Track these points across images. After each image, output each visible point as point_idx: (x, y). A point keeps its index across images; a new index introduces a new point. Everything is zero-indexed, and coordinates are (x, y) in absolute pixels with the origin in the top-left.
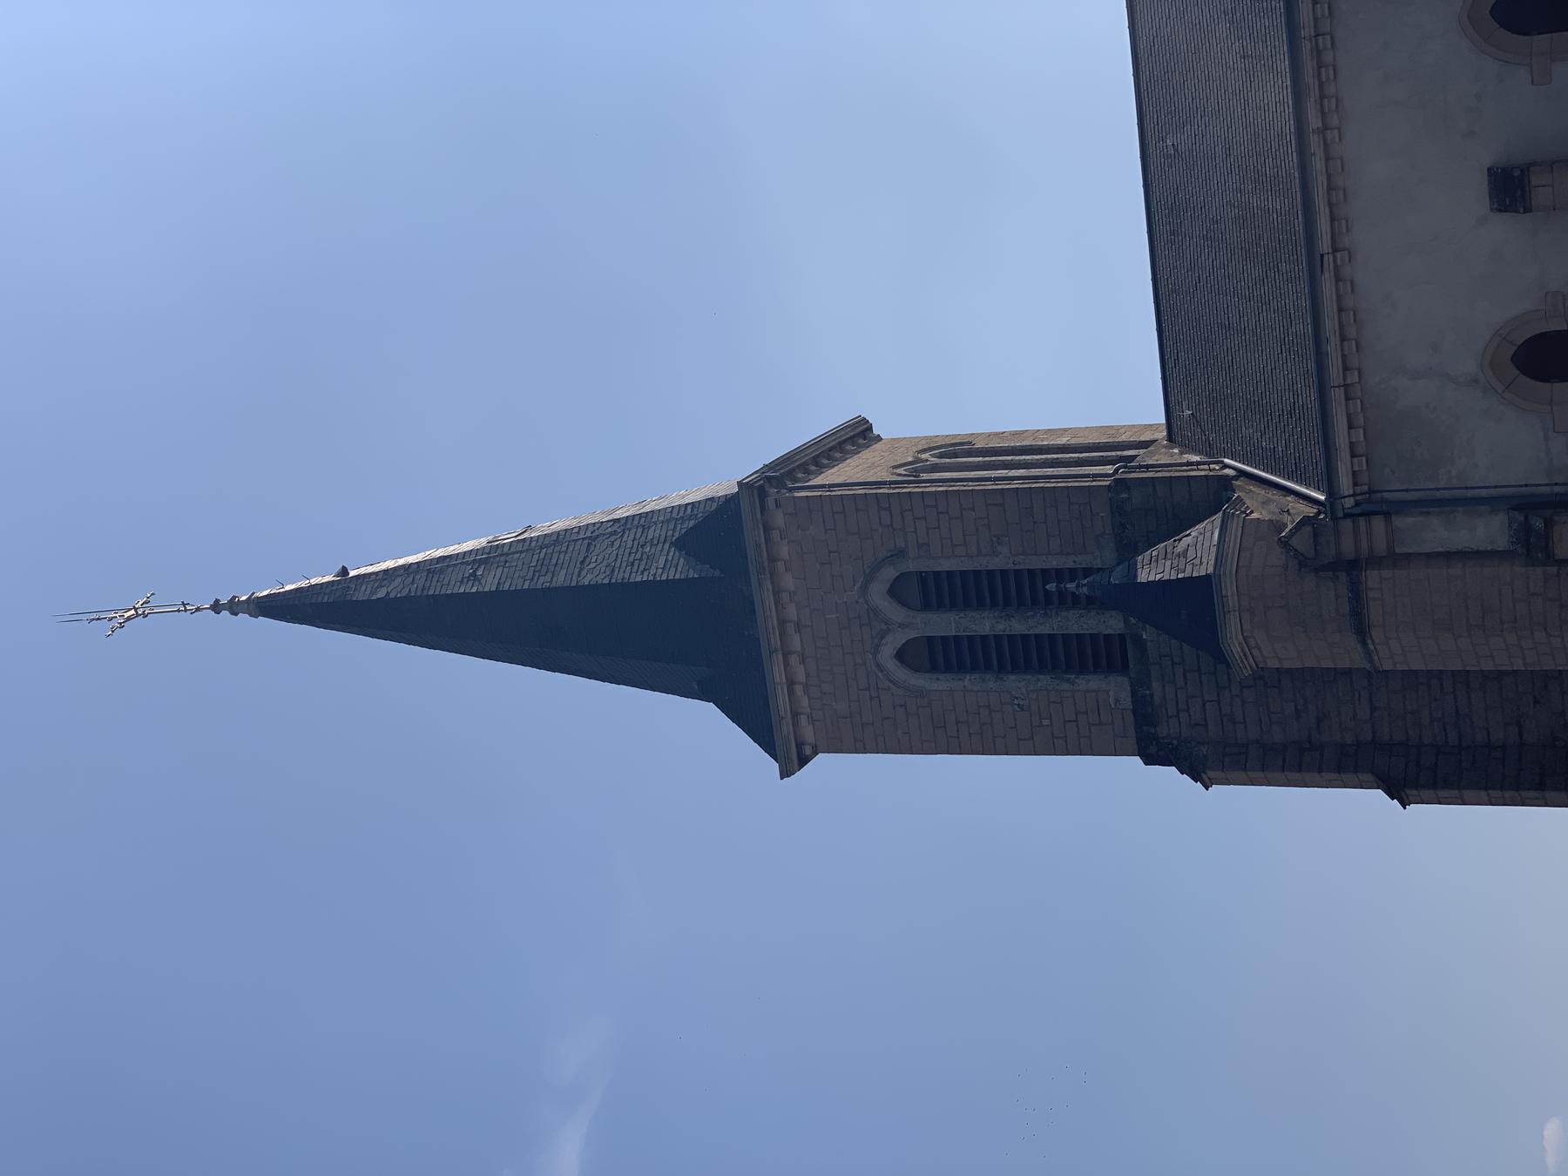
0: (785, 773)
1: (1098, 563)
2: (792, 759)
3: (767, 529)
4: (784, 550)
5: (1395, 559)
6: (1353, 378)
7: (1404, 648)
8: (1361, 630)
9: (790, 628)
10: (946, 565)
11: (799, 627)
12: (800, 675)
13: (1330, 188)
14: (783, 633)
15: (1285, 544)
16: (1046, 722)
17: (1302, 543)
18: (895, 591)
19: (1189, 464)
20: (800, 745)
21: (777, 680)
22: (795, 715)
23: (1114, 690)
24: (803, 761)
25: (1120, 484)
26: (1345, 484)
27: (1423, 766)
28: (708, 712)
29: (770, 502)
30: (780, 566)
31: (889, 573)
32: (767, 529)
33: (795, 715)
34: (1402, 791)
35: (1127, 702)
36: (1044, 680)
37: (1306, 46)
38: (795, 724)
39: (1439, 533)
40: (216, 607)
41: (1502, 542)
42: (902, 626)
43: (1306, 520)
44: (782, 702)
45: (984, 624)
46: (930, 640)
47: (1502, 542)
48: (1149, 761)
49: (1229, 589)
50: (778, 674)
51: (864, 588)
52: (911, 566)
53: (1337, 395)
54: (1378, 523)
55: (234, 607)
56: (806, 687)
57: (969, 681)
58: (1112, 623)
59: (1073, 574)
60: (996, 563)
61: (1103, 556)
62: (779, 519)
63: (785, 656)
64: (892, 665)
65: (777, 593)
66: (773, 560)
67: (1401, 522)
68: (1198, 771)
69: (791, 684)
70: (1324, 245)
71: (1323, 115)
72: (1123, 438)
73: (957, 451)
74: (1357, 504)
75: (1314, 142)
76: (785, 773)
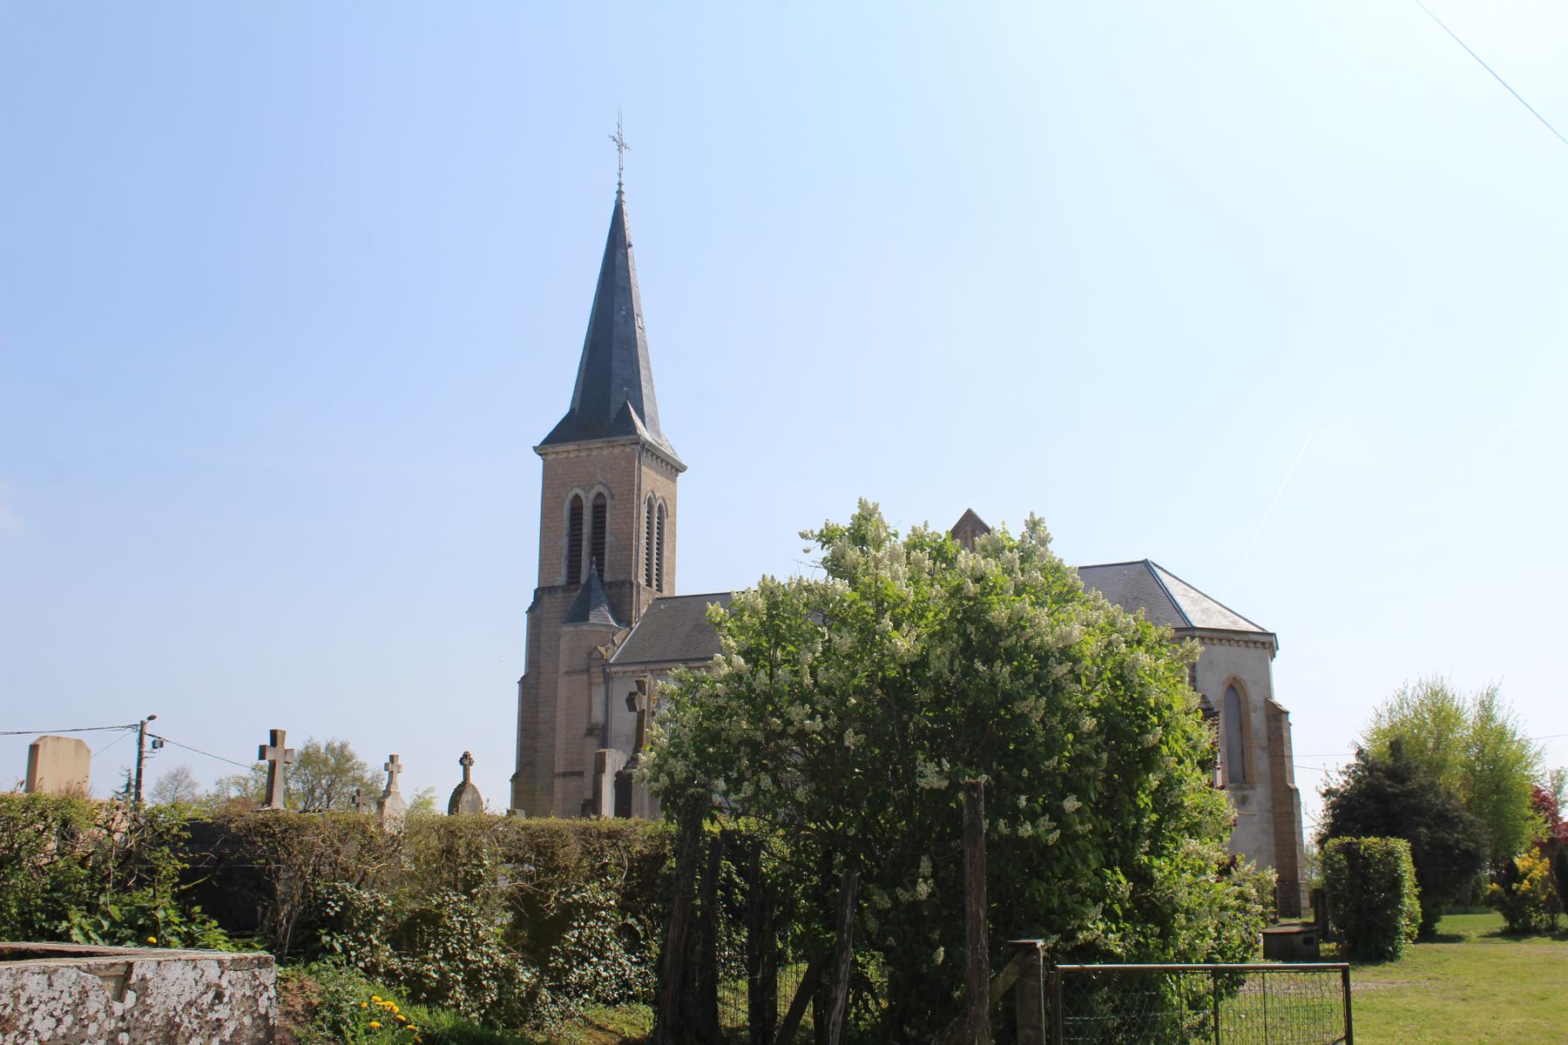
4: (616, 451)
5: (590, 685)
7: (563, 687)
8: (568, 673)
17: (596, 655)
18: (600, 495)
23: (561, 580)
26: (614, 669)
27: (531, 689)
28: (564, 409)
31: (606, 493)
34: (523, 682)
36: (565, 552)
40: (620, 184)
44: (561, 448)
45: (587, 530)
47: (594, 720)
48: (536, 591)
49: (585, 627)
50: (571, 447)
52: (608, 502)
53: (642, 667)
55: (620, 193)
58: (583, 579)
60: (607, 535)
61: (607, 577)
62: (628, 449)
67: (602, 689)
68: (531, 610)
72: (665, 578)
73: (660, 516)
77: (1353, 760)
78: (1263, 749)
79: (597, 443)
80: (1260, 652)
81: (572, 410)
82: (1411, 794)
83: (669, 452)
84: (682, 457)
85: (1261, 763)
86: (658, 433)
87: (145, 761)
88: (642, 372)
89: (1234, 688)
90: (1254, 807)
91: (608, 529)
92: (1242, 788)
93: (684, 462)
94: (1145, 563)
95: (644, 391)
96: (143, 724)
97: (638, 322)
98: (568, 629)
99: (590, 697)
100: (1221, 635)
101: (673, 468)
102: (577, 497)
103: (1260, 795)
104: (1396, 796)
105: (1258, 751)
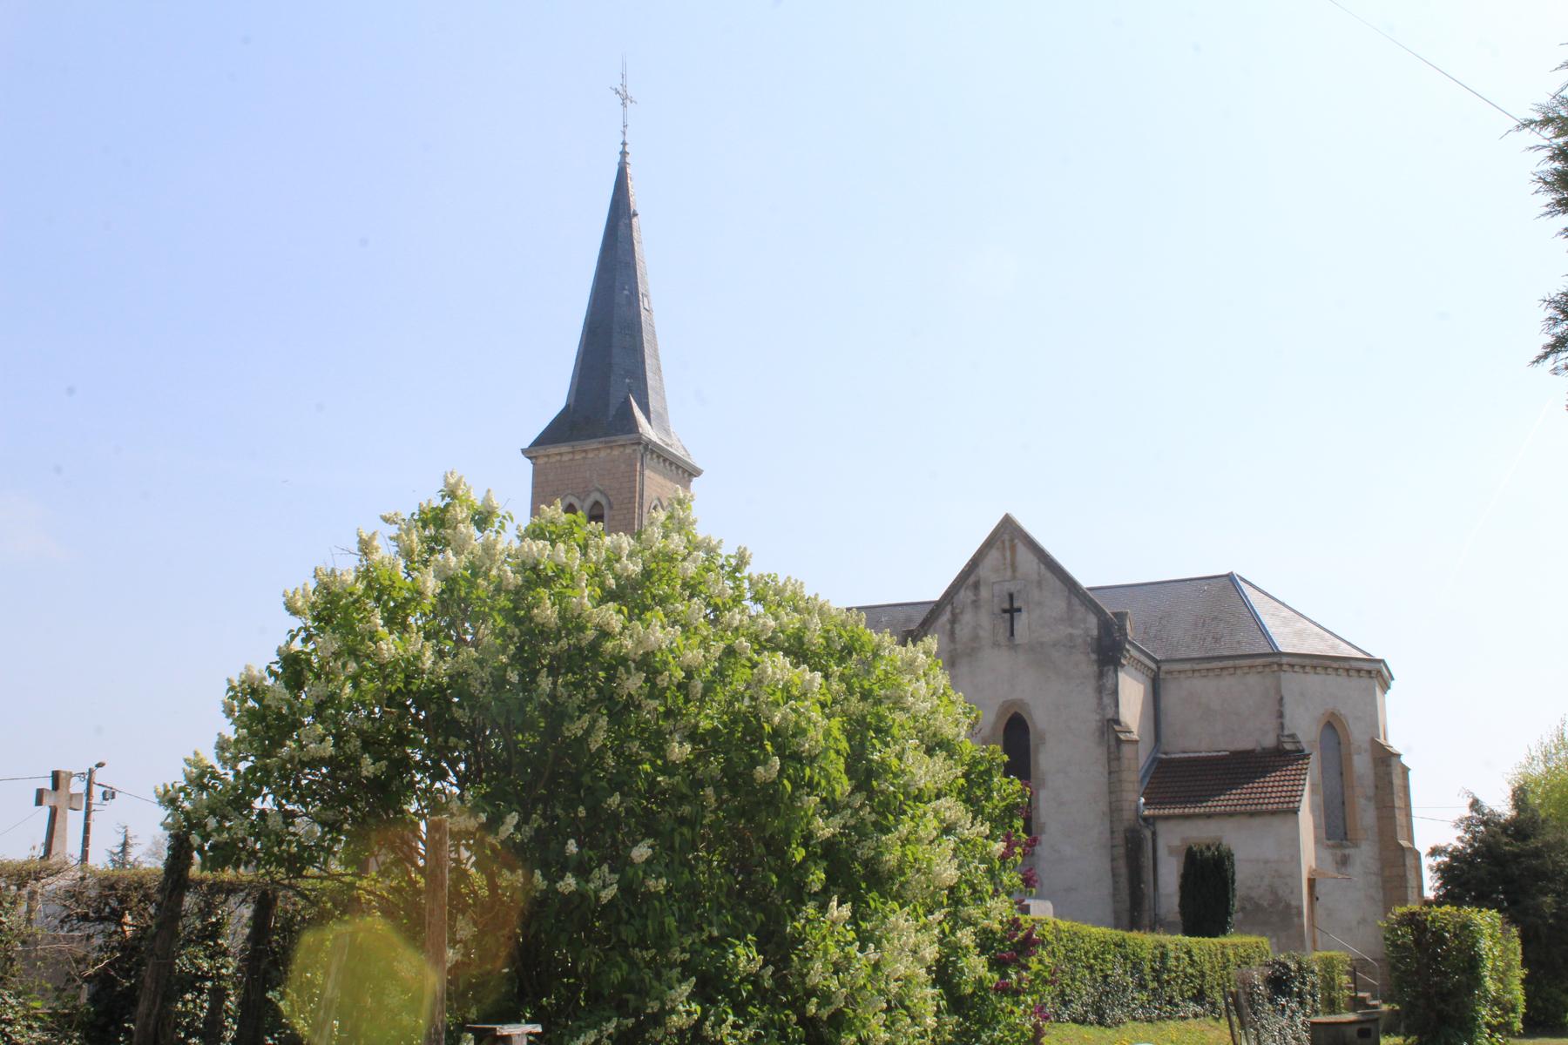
0: (524, 451)
4: (616, 452)
12: (565, 458)
18: (597, 503)
31: (604, 502)
40: (624, 144)
44: (552, 450)
50: (564, 448)
52: (606, 512)
55: (624, 154)
62: (628, 451)
76: (524, 451)
77: (1467, 813)
78: (1368, 799)
79: (593, 444)
80: (1365, 682)
81: (567, 406)
82: (1537, 853)
83: (680, 453)
84: (696, 460)
85: (1365, 815)
86: (667, 432)
87: (93, 815)
88: (649, 362)
89: (1332, 726)
90: (1356, 870)
92: (1341, 846)
93: (699, 465)
94: (1230, 577)
95: (650, 382)
96: (91, 772)
97: (644, 303)
100: (1315, 662)
101: (686, 472)
103: (1365, 854)
104: (1516, 856)
105: (1362, 801)
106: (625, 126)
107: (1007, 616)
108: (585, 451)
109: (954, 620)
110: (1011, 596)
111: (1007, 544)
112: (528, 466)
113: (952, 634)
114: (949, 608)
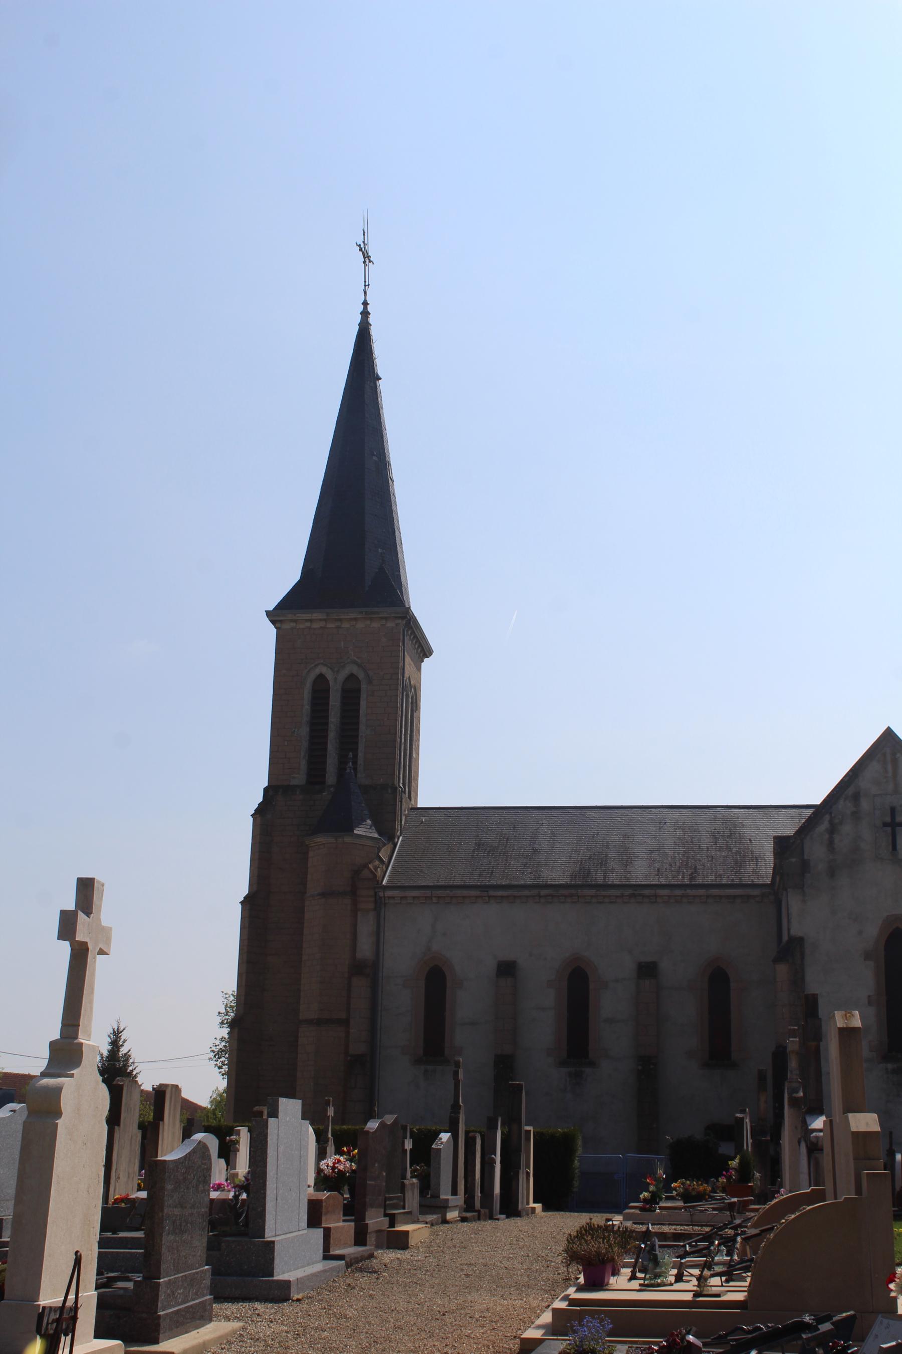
0: (268, 613)
1: (359, 775)
2: (274, 616)
3: (386, 618)
4: (375, 625)
6: (434, 900)
8: (323, 895)
9: (338, 624)
10: (363, 703)
11: (338, 628)
12: (316, 625)
13: (515, 897)
14: (336, 620)
15: (366, 866)
16: (286, 743)
17: (365, 873)
18: (352, 677)
19: (401, 820)
20: (281, 621)
21: (314, 615)
22: (296, 621)
23: (299, 778)
24: (273, 622)
25: (395, 789)
26: (389, 893)
29: (399, 621)
30: (368, 622)
31: (361, 675)
32: (386, 618)
33: (296, 621)
35: (294, 782)
36: (305, 744)
37: (573, 891)
38: (292, 621)
39: (366, 928)
40: (365, 304)
41: (359, 955)
42: (336, 678)
43: (375, 876)
45: (334, 718)
46: (328, 691)
47: (359, 955)
48: (266, 790)
49: (348, 839)
50: (316, 615)
51: (355, 662)
52: (364, 686)
53: (428, 893)
54: (371, 906)
55: (365, 314)
56: (309, 628)
57: (307, 708)
58: (331, 778)
59: (355, 763)
60: (362, 727)
62: (390, 624)
63: (325, 620)
64: (317, 671)
65: (355, 619)
66: (371, 619)
68: (259, 813)
69: (311, 621)
70: (492, 893)
71: (546, 896)
72: (413, 783)
74: (380, 898)
75: (534, 892)
76: (268, 613)
91: (363, 719)
98: (320, 839)
99: (355, 926)
102: (321, 677)
106: (366, 286)
107: (889, 829)
108: (340, 620)
109: (833, 830)
110: (893, 811)
111: (889, 758)
112: (271, 632)
113: (831, 843)
114: (827, 817)
